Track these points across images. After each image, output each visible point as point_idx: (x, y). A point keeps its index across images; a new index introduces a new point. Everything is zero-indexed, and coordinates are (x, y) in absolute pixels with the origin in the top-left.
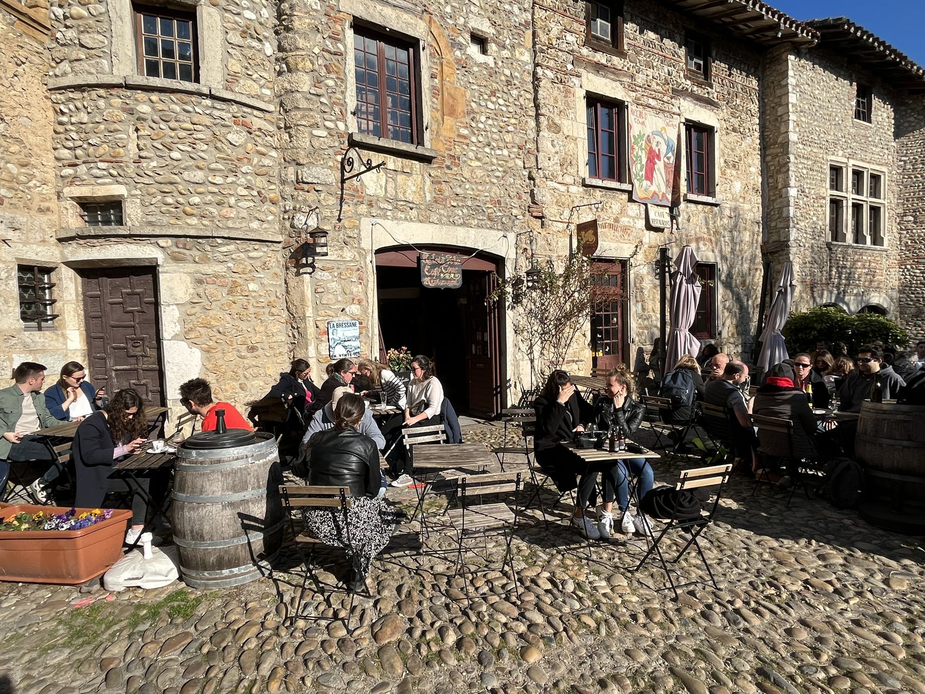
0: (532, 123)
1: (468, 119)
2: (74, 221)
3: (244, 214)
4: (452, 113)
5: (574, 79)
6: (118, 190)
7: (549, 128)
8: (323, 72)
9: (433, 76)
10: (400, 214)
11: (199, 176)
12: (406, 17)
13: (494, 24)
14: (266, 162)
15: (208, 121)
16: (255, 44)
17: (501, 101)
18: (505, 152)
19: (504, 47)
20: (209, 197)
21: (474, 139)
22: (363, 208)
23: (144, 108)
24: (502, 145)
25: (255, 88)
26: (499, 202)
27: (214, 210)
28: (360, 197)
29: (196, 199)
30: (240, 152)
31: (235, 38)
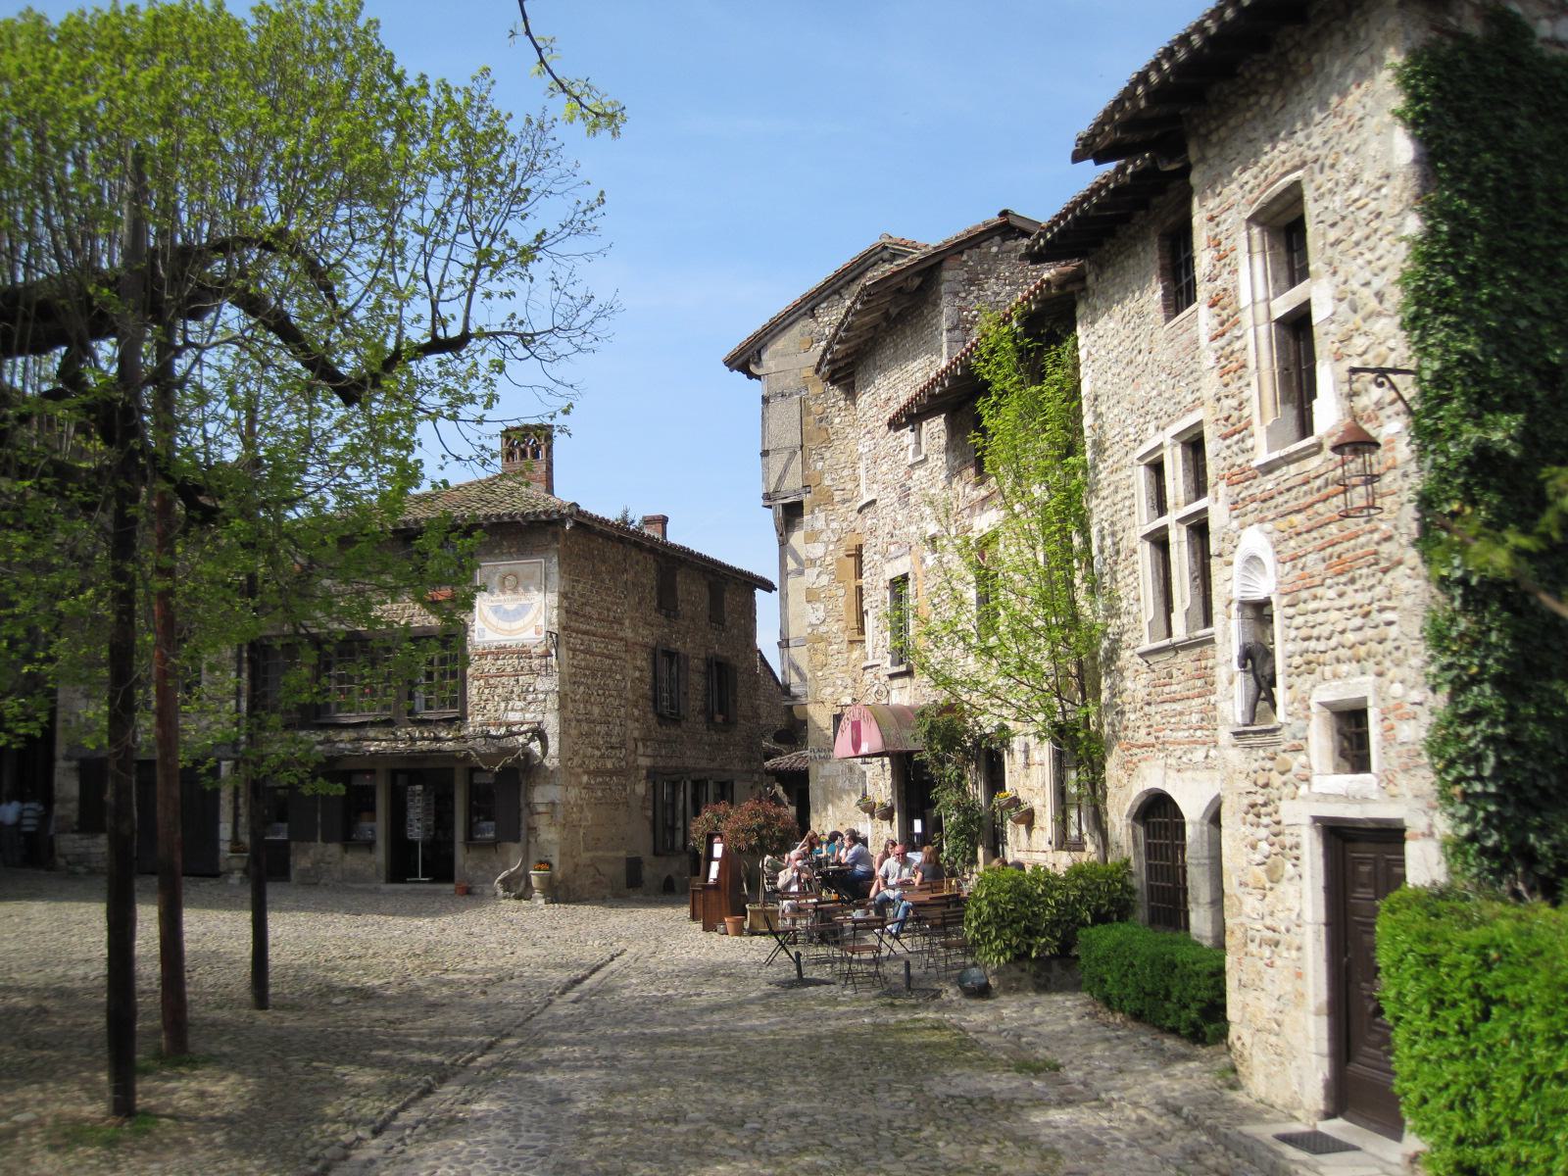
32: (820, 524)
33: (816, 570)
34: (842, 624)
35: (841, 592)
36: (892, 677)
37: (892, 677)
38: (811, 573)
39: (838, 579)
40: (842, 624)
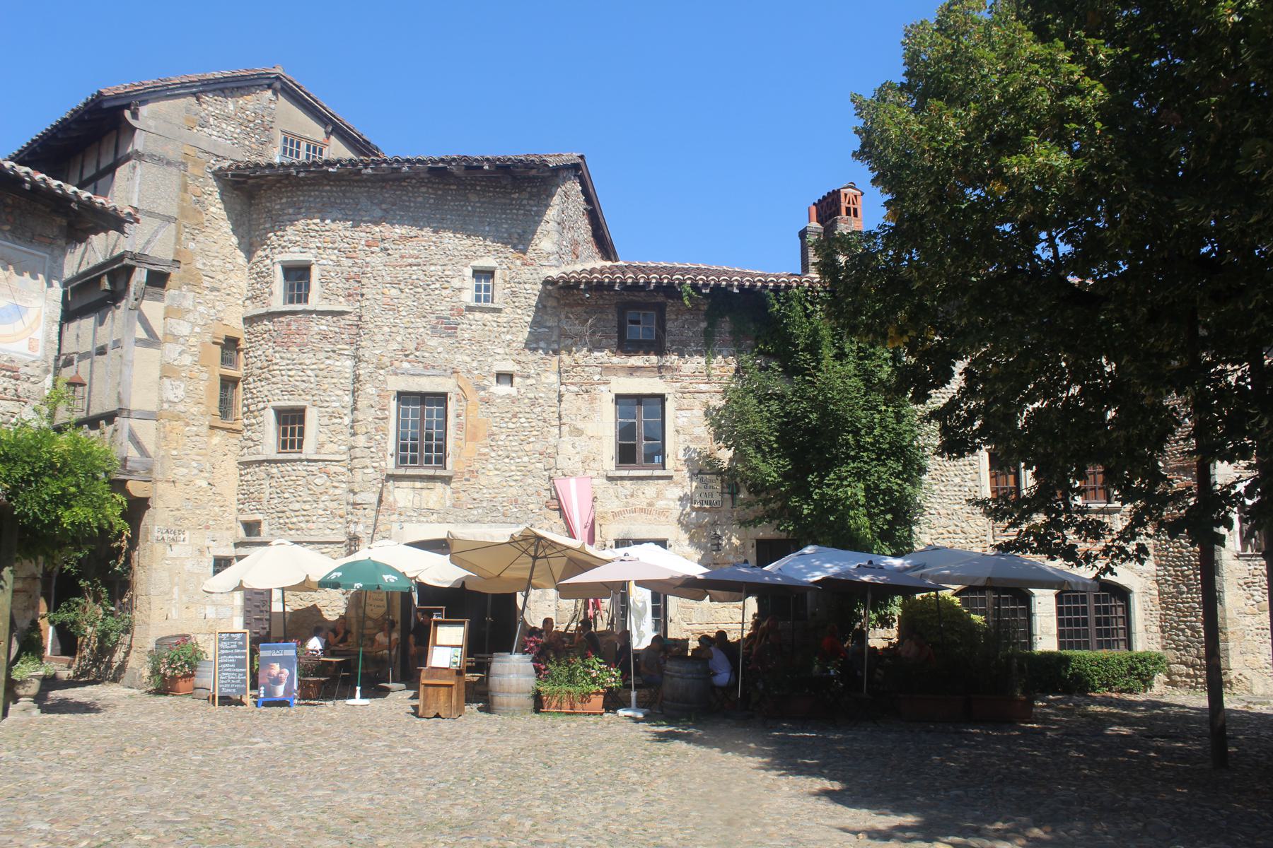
0: (557, 431)
1: (488, 441)
2: (242, 534)
3: (321, 525)
4: (474, 438)
5: (602, 387)
6: (259, 517)
7: (571, 433)
8: (373, 431)
9: (458, 416)
10: (422, 519)
11: (296, 506)
12: (437, 379)
13: (519, 363)
14: (337, 491)
15: (304, 474)
16: (338, 421)
17: (523, 420)
18: (526, 459)
19: (528, 377)
20: (301, 518)
21: (493, 454)
22: (395, 517)
23: (274, 470)
24: (520, 453)
25: (335, 447)
26: (516, 501)
27: (303, 525)
28: (392, 509)
29: (295, 520)
30: (322, 489)
31: (325, 421)
32: (188, 304)
33: (179, 348)
34: (202, 408)
35: (205, 376)
36: (391, 477)
37: (391, 477)
38: (171, 351)
39: (201, 362)
40: (202, 408)
